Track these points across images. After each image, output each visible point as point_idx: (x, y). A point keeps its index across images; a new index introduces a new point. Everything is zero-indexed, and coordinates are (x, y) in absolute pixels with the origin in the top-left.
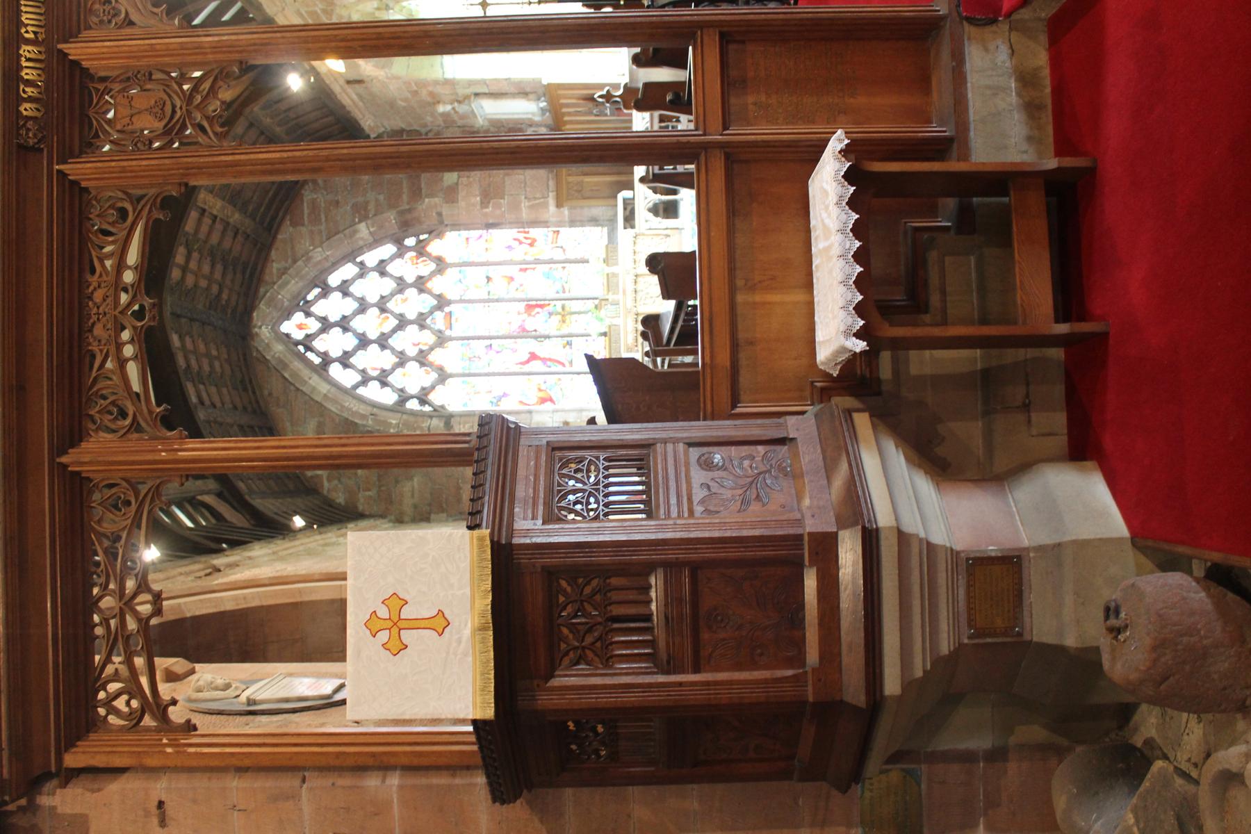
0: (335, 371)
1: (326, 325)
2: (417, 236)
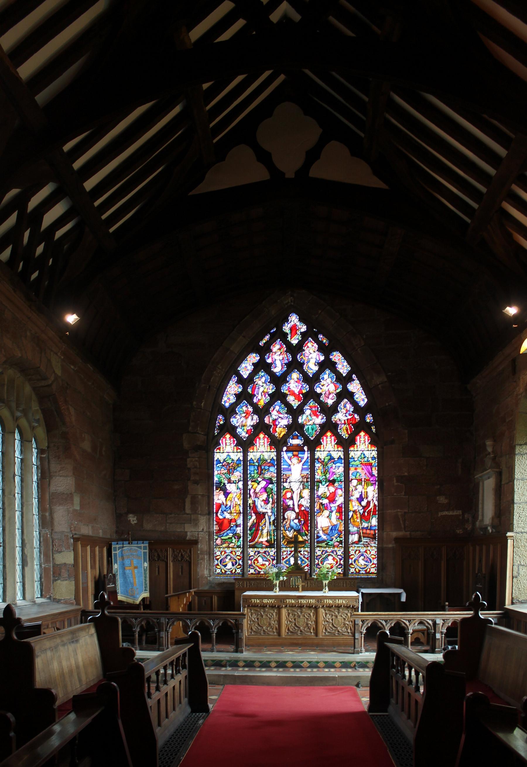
1: (295, 350)
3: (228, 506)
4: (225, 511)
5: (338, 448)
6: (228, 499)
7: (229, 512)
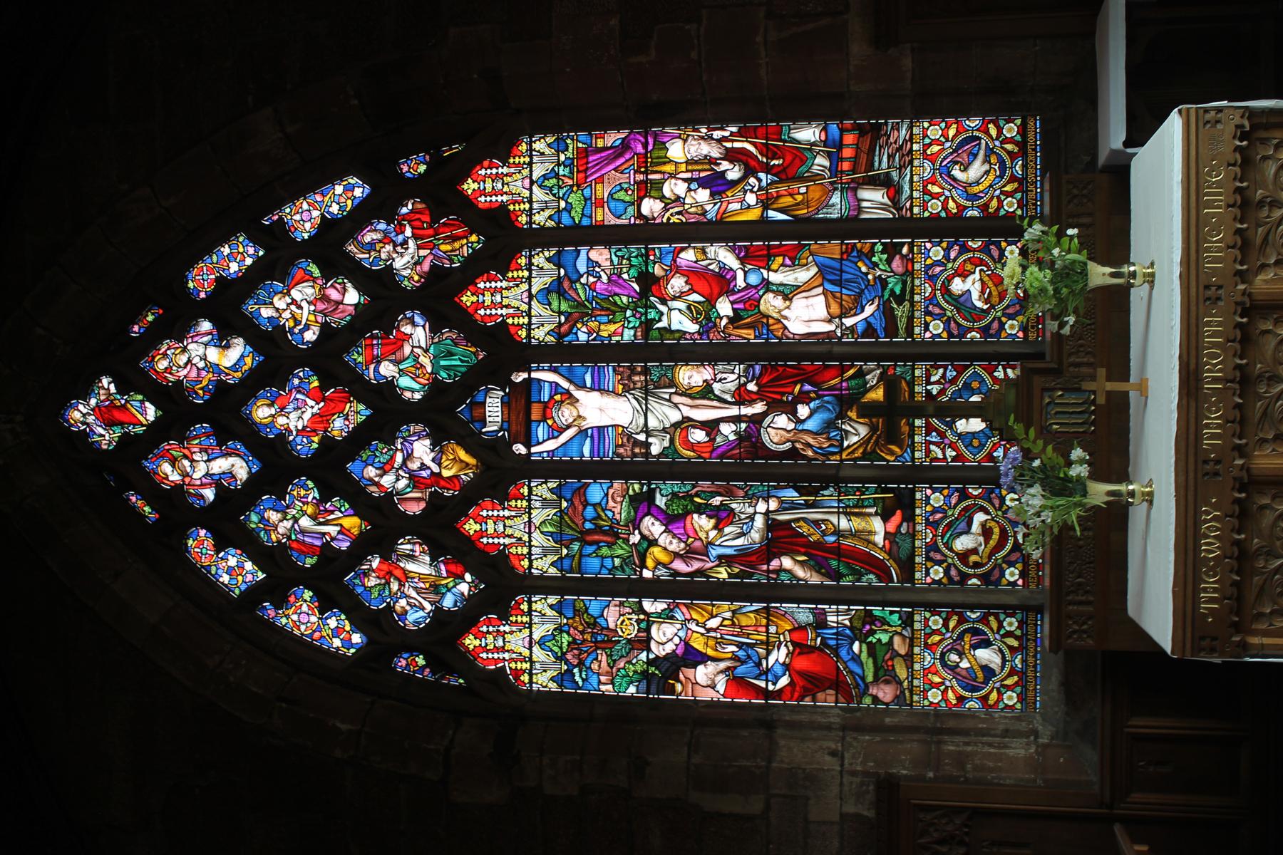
0: (200, 544)
2: (431, 147)
3: (741, 654)
4: (759, 664)
5: (519, 268)
6: (710, 652)
7: (762, 651)
